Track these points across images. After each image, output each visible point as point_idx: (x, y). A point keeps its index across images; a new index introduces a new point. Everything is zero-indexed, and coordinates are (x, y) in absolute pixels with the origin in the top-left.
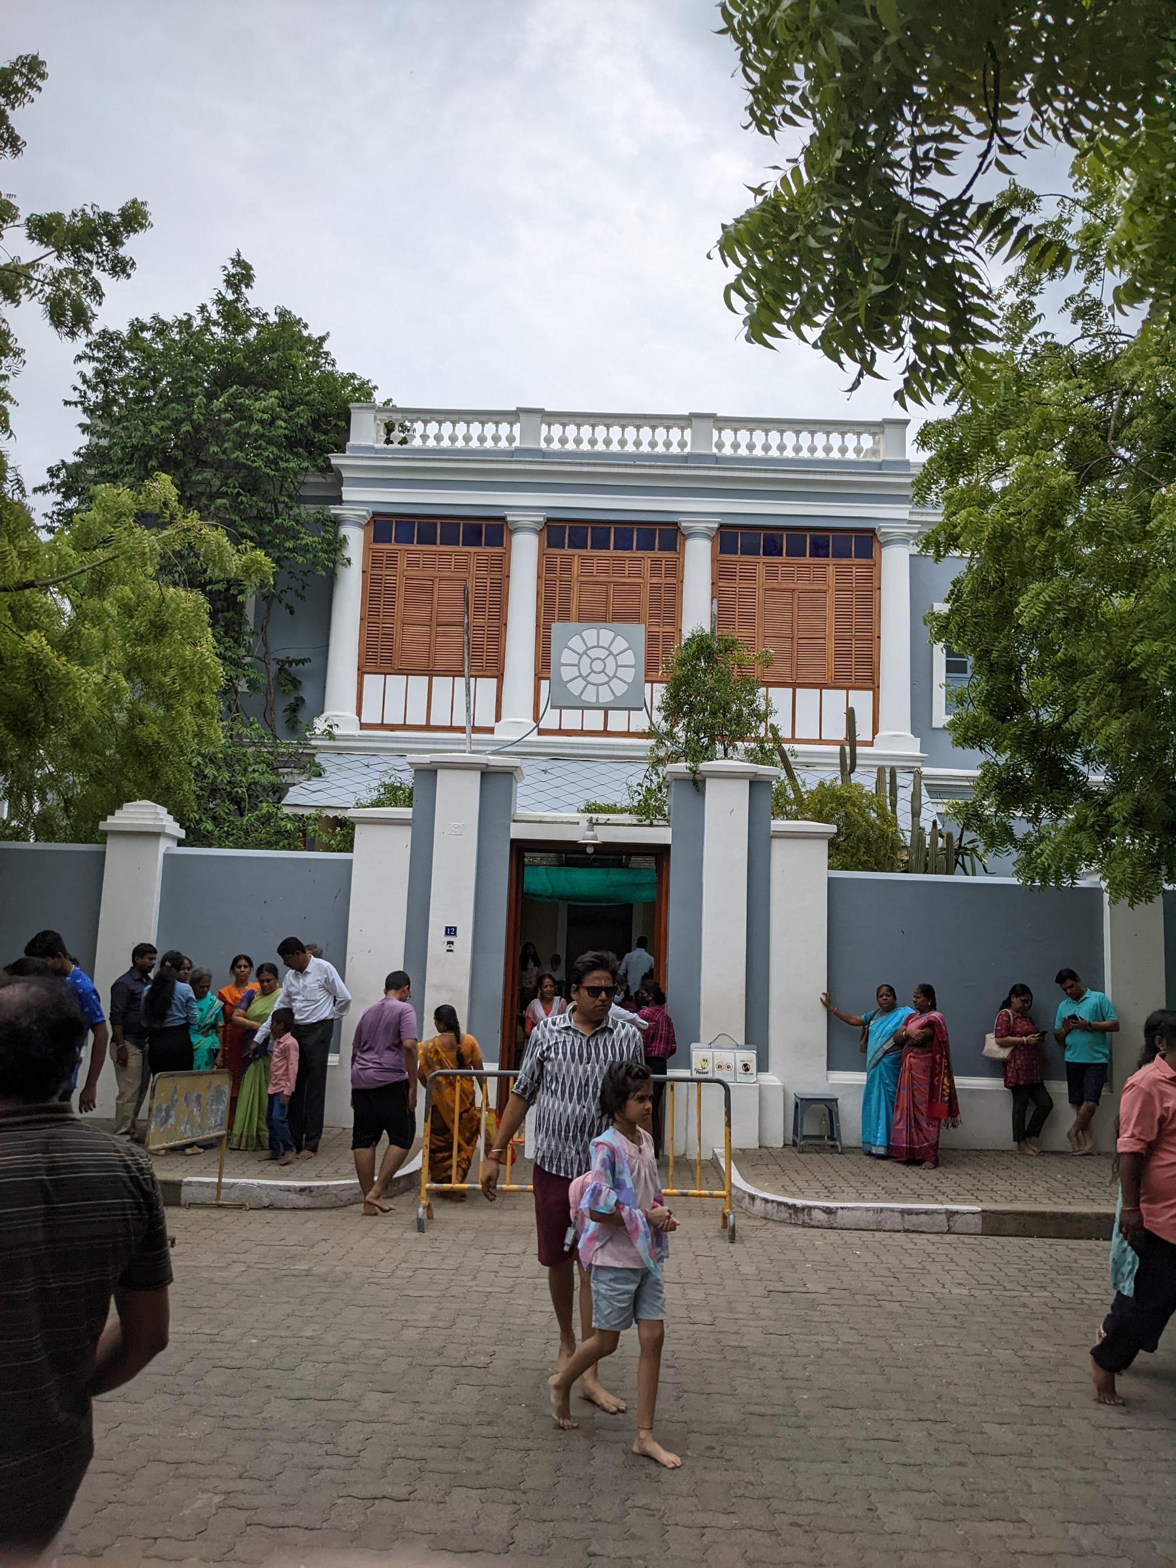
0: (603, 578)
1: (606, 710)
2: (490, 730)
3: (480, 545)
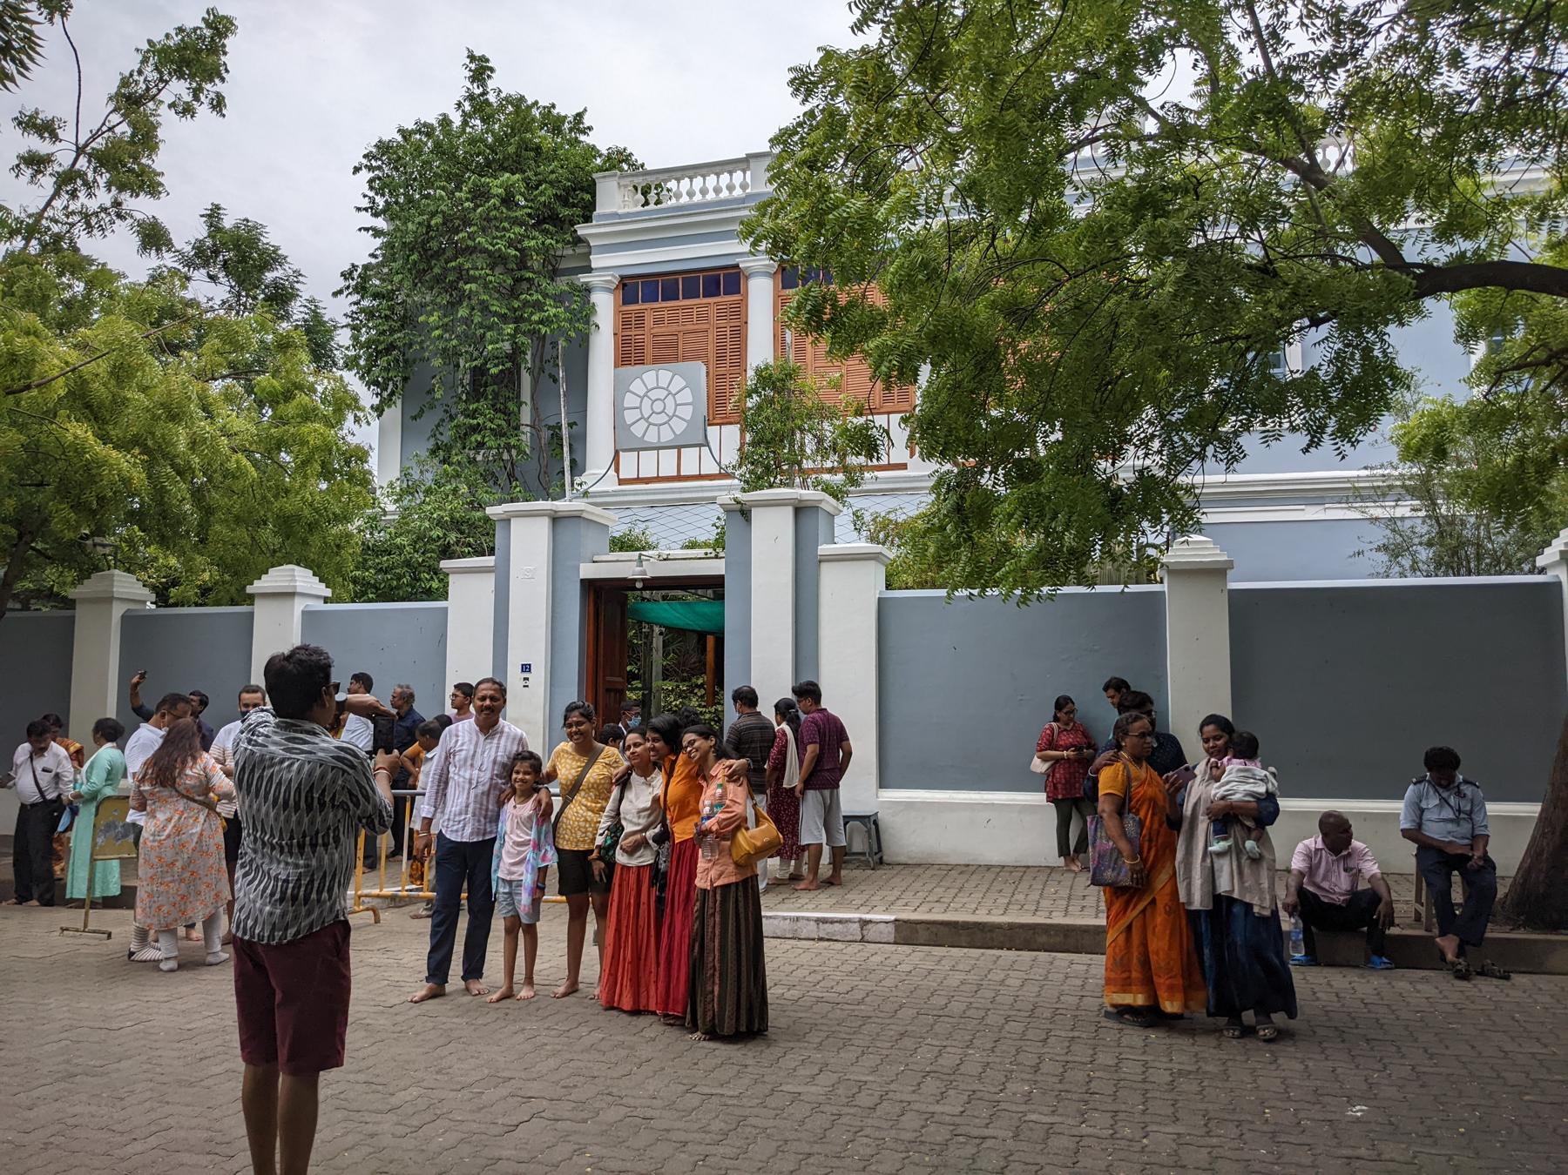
1: (679, 448)
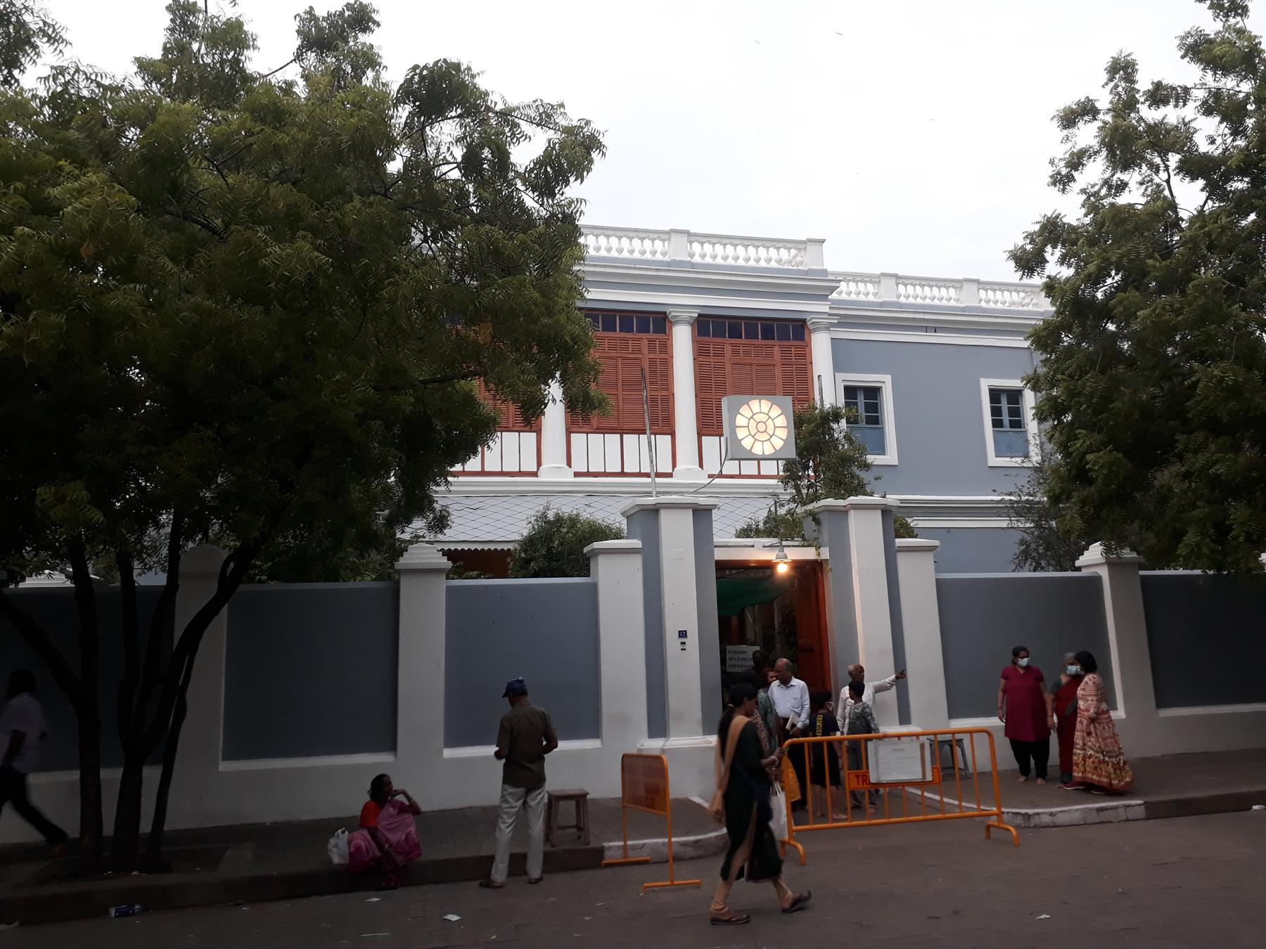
0: (613, 353)
2: (535, 474)
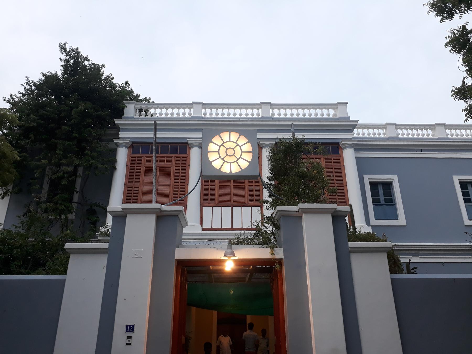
3: (176, 153)
